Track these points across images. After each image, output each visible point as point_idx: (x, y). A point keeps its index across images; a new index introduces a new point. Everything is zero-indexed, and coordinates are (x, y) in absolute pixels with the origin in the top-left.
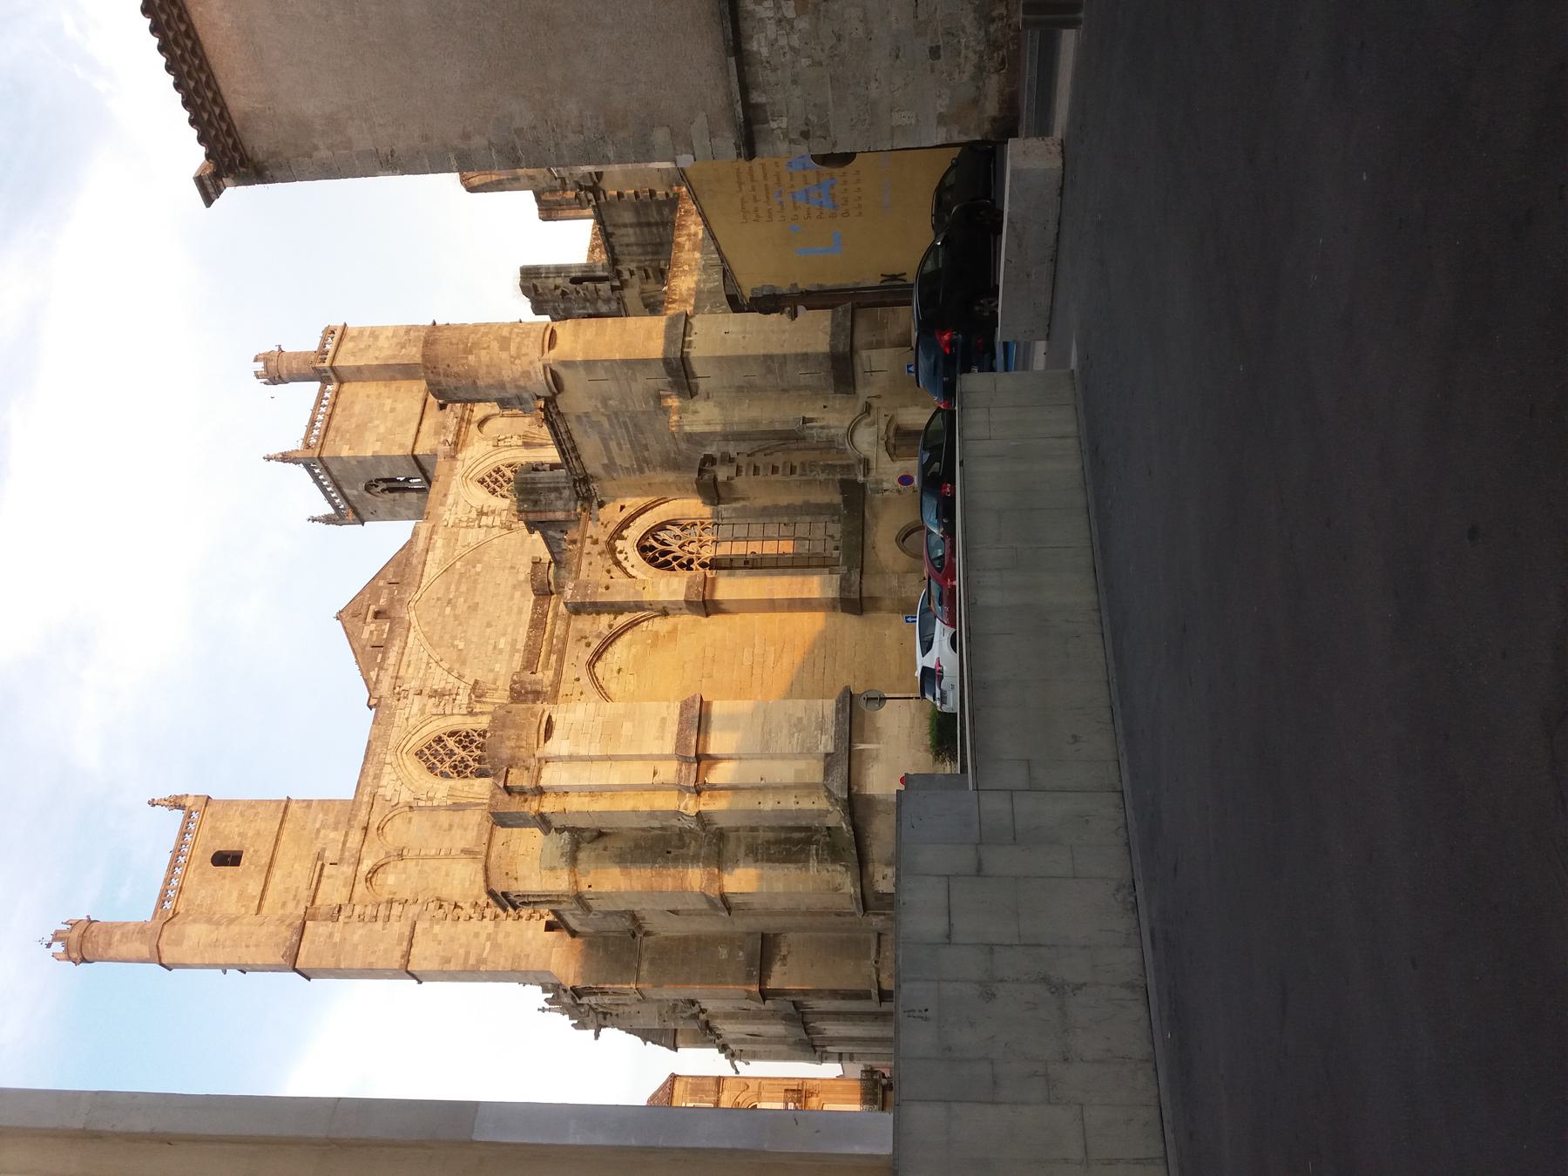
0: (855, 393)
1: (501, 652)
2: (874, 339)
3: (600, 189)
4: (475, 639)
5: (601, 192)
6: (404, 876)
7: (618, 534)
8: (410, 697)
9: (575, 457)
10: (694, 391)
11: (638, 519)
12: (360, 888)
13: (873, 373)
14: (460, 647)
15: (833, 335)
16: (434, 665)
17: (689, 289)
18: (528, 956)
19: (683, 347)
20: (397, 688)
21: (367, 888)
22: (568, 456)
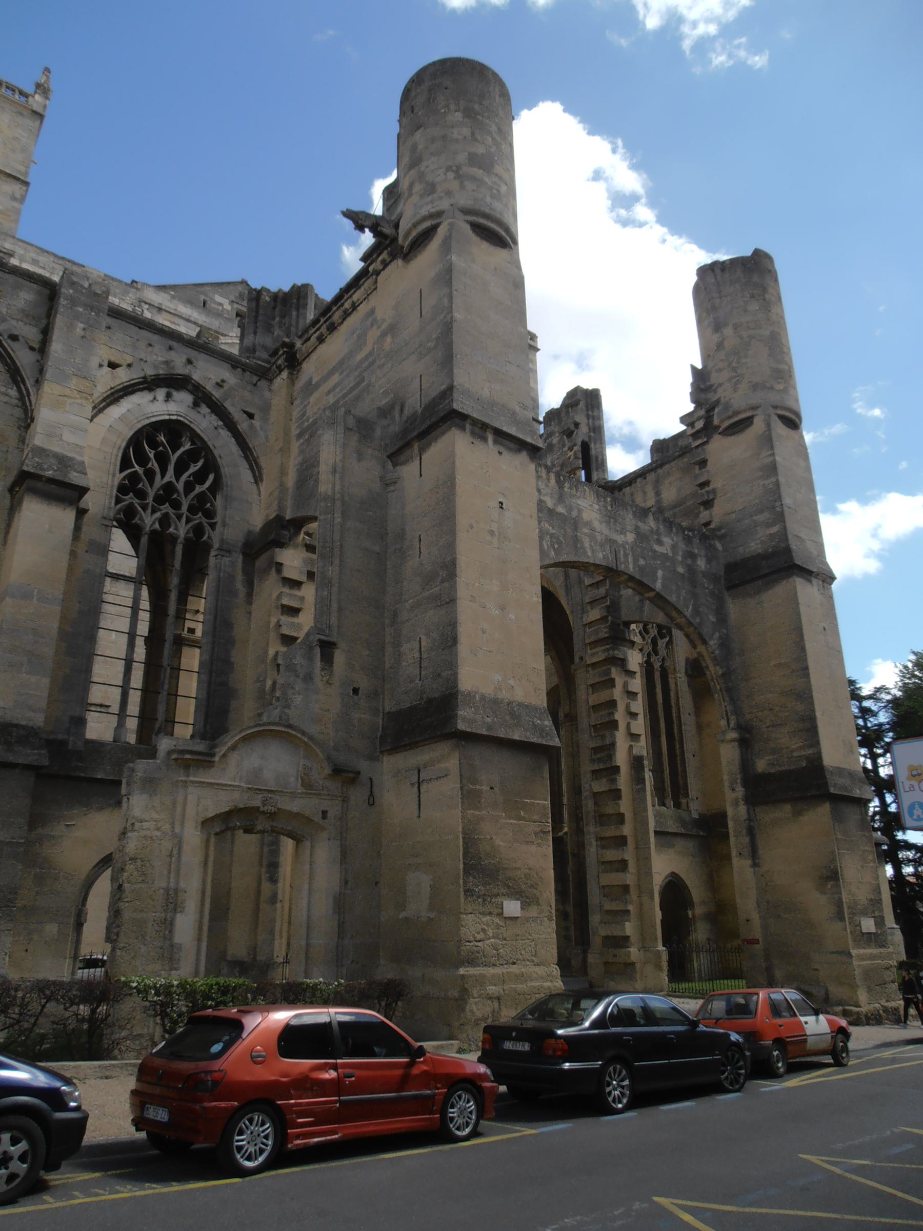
0: (382, 752)
2: (485, 788)
3: (709, 437)
5: (705, 440)
7: (201, 397)
9: (322, 335)
10: (402, 458)
11: (230, 434)
13: (415, 789)
15: (494, 704)
17: (580, 511)
19: (475, 422)
20: (147, 306)
22: (322, 320)
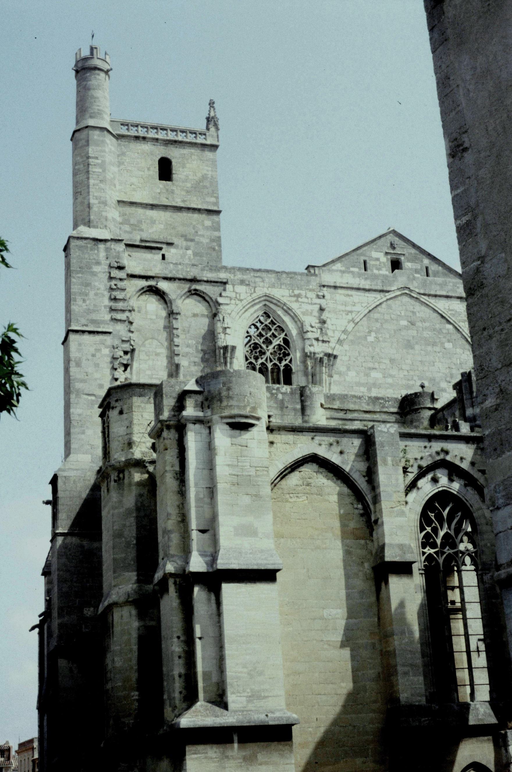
1: (367, 375)
4: (377, 350)
6: (154, 317)
8: (318, 301)
12: (144, 283)
14: (368, 337)
16: (350, 317)
18: (83, 433)
21: (143, 288)
